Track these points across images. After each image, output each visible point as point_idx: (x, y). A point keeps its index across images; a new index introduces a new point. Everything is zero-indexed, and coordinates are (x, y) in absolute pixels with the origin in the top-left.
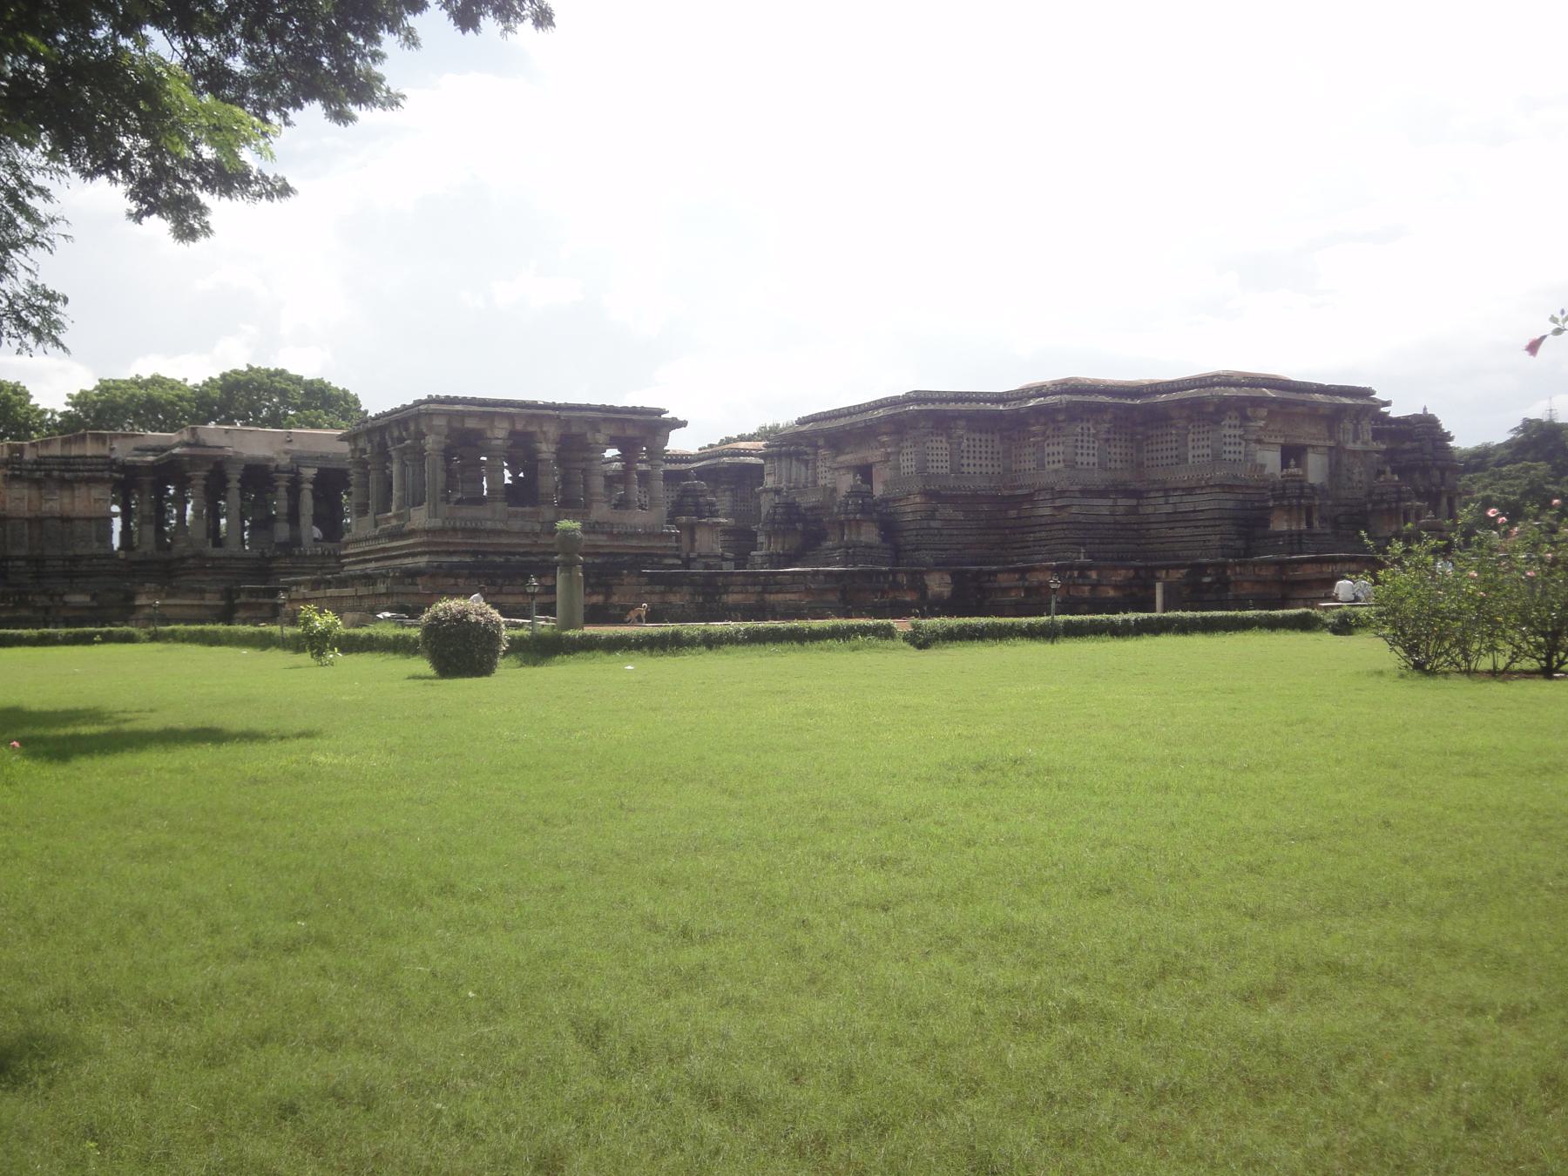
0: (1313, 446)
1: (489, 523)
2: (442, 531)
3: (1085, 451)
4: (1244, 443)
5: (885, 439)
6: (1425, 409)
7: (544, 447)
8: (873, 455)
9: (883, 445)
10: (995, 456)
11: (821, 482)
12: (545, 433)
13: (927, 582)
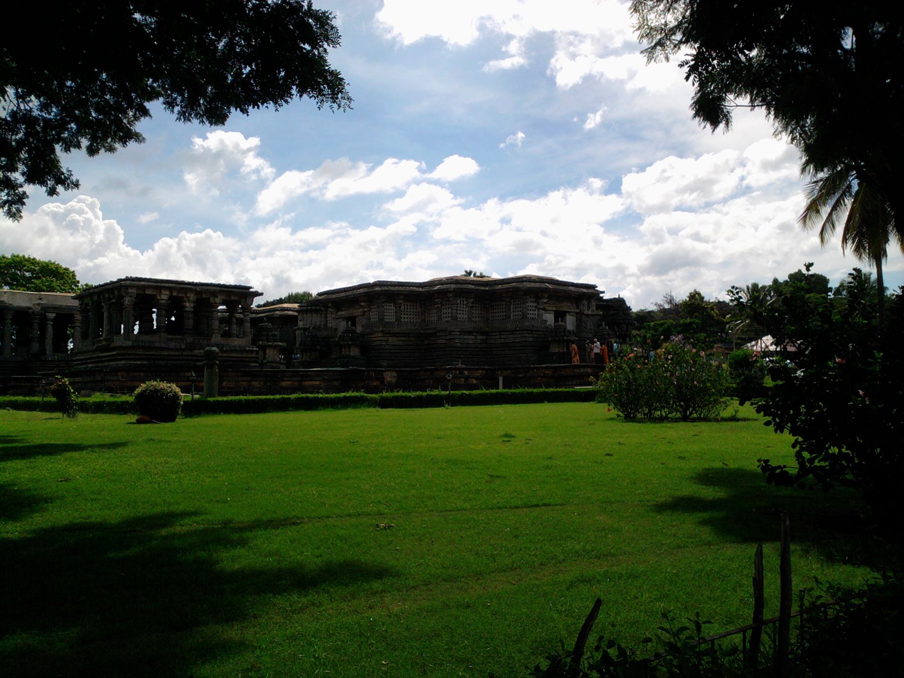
0: (568, 312)
2: (132, 348)
3: (462, 312)
4: (537, 310)
5: (363, 304)
7: (187, 304)
8: (357, 312)
9: (362, 307)
11: (329, 325)
12: (188, 297)
13: (384, 376)
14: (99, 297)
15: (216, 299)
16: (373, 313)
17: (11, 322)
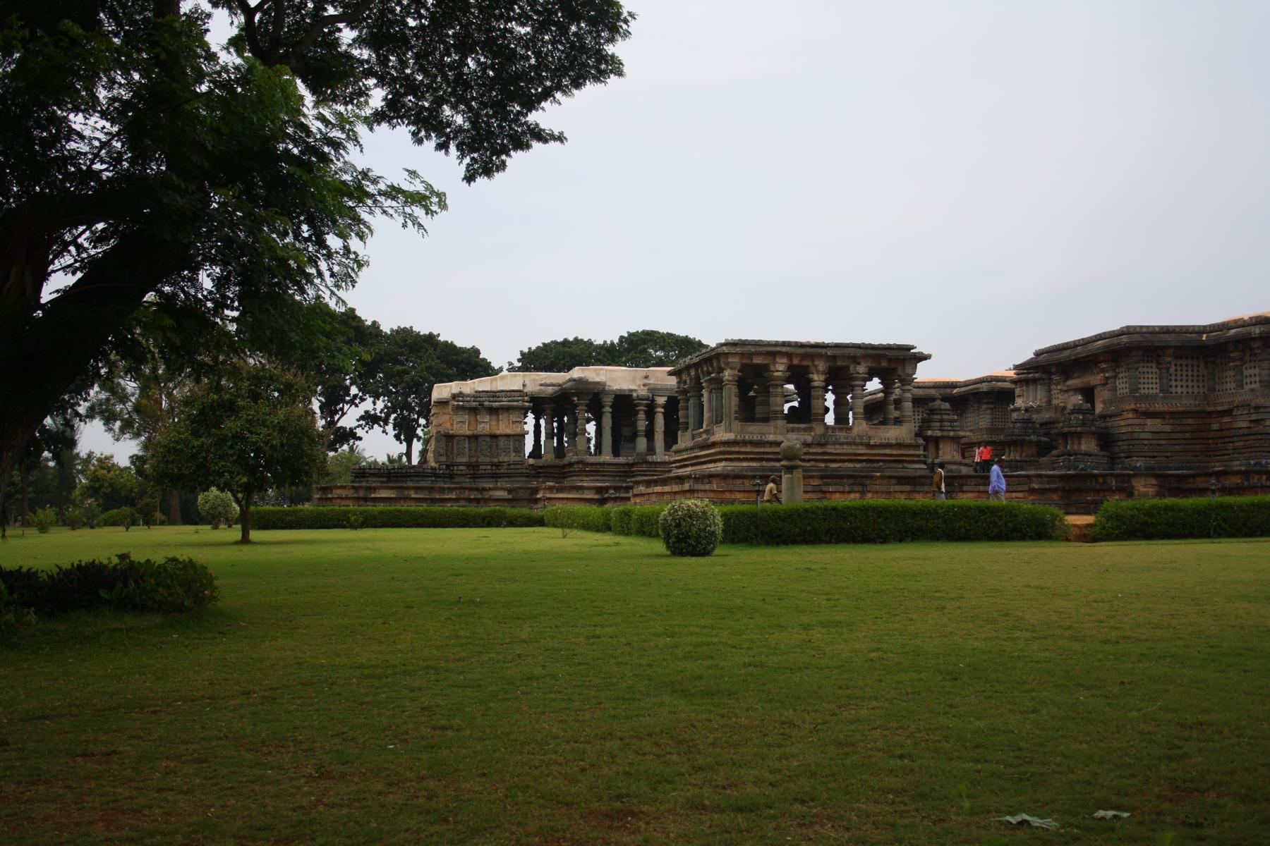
1: (771, 436)
5: (1104, 366)
7: (815, 377)
8: (1095, 379)
9: (1103, 371)
10: (1201, 378)
11: (1055, 402)
12: (815, 366)
13: (1133, 483)
16: (1121, 381)
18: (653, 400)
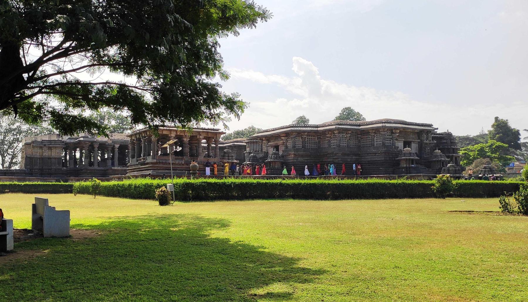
0: (413, 141)
2: (156, 163)
4: (392, 140)
6: (448, 130)
7: (185, 139)
9: (282, 140)
11: (264, 150)
14: (139, 136)
15: (200, 136)
17: (118, 150)
18: (114, 146)
